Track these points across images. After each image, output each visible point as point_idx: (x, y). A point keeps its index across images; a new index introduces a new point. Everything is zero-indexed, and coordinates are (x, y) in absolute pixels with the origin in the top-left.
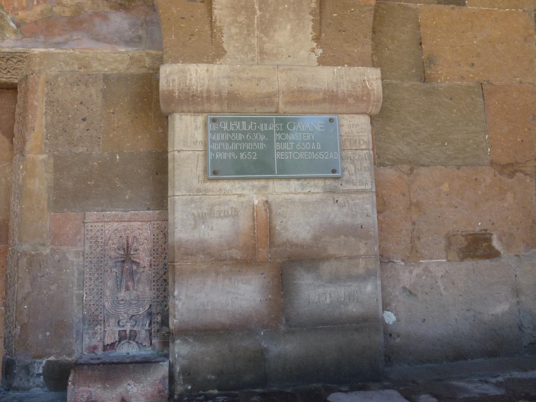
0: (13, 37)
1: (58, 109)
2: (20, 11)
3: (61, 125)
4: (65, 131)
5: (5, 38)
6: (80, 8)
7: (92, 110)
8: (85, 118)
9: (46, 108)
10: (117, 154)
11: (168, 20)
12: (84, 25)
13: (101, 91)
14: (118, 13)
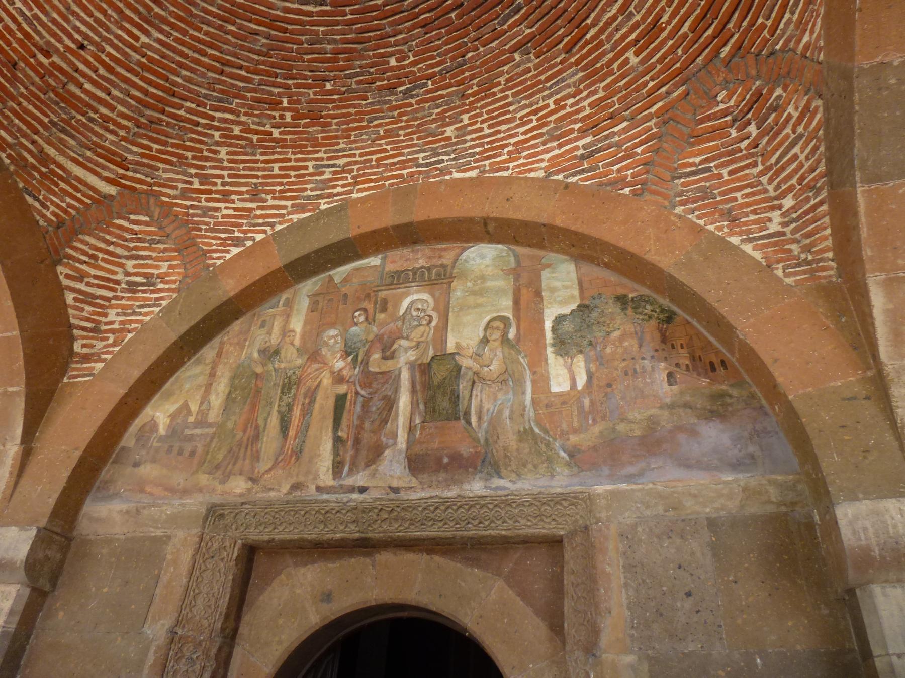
0: (566, 471)
1: (644, 578)
3: (653, 604)
4: (661, 615)
5: (555, 474)
6: (653, 423)
8: (690, 591)
9: (625, 577)
10: (757, 656)
11: (820, 431)
14: (711, 424)
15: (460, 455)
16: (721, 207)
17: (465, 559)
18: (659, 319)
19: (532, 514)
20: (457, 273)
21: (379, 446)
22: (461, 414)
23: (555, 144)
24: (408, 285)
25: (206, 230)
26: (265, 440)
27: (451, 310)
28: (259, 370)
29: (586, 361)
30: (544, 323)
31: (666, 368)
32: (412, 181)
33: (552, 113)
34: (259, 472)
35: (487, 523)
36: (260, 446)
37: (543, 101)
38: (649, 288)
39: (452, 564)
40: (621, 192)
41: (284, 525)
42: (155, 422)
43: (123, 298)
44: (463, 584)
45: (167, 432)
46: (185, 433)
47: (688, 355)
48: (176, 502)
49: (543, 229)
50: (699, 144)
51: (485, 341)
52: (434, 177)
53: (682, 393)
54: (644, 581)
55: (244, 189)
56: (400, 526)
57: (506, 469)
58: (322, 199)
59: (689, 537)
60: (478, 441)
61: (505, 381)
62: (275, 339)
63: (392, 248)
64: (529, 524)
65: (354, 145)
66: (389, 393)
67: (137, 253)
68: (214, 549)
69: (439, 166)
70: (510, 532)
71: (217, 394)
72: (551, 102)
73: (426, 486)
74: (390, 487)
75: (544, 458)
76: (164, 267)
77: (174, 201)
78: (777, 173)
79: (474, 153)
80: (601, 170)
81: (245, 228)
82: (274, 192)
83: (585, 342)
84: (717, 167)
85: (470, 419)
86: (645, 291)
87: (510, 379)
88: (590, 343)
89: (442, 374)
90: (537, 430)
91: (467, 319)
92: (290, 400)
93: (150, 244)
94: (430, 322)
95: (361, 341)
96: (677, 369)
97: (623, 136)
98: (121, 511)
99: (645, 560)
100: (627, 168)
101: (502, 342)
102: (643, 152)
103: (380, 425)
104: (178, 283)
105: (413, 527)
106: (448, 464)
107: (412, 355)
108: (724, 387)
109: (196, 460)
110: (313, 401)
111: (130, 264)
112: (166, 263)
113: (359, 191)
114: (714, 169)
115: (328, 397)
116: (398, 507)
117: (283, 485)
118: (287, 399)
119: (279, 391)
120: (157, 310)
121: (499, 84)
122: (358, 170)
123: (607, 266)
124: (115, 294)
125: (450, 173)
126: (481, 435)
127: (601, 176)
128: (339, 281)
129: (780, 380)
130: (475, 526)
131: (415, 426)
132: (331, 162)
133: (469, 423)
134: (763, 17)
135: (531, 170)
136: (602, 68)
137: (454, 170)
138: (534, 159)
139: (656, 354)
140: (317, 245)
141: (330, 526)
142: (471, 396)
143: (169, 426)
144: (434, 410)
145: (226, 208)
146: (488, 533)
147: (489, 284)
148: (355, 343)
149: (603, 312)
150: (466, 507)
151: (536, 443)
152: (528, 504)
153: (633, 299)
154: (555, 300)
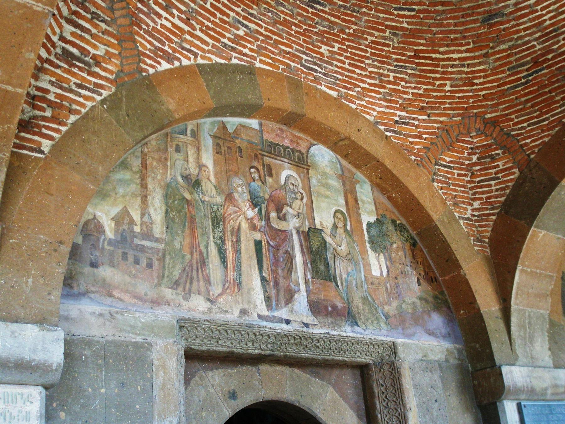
23: (385, 104)
25: (146, 32)
26: (211, 266)
28: (188, 196)
33: (390, 83)
36: (207, 271)
37: (388, 71)
38: (408, 221)
39: (304, 375)
42: (98, 221)
43: (58, 67)
44: (312, 388)
45: (115, 235)
46: (135, 242)
50: (453, 152)
51: (335, 226)
55: (183, 8)
60: (344, 299)
65: (262, 17)
66: (289, 249)
67: (77, 19)
69: (315, 74)
71: (155, 210)
72: (392, 75)
75: (375, 317)
76: (101, 51)
78: (477, 187)
81: (174, 45)
82: (202, 24)
86: (404, 222)
90: (370, 299)
91: (323, 205)
92: (221, 234)
93: (93, 18)
94: (302, 199)
97: (421, 124)
100: (417, 143)
103: (287, 273)
104: (114, 75)
109: (155, 274)
110: (239, 241)
111: (68, 28)
112: (102, 47)
113: (261, 61)
117: (234, 310)
119: (210, 224)
120: (99, 98)
121: (366, 39)
122: (262, 41)
123: (390, 198)
124: (48, 56)
125: (321, 85)
126: (344, 295)
129: (478, 301)
132: (246, 22)
133: (337, 285)
134: (516, 116)
135: (368, 113)
136: (429, 78)
137: (323, 83)
138: (370, 106)
142: (335, 266)
143: (116, 231)
145: (166, 18)
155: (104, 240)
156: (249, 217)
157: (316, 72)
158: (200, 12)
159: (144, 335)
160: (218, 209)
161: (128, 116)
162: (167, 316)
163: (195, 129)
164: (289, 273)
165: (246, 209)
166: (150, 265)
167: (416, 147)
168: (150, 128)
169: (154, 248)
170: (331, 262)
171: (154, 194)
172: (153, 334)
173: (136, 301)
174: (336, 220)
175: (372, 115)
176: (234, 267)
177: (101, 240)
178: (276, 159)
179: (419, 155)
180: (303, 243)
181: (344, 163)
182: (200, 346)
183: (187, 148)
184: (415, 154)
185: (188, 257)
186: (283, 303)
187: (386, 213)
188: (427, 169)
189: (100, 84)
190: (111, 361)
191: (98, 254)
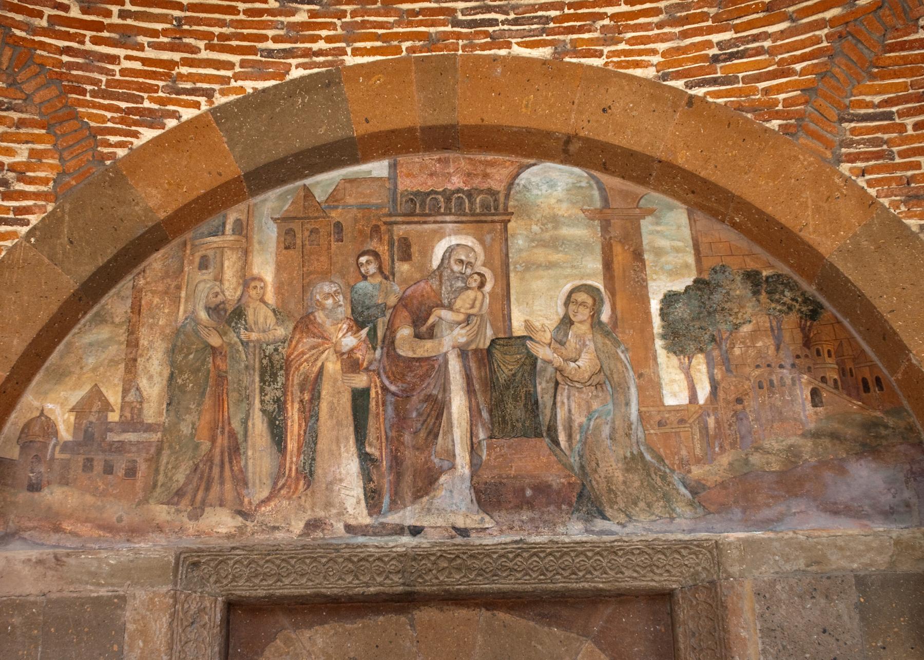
0: (688, 512)
1: (784, 644)
2: (693, 465)
5: (675, 515)
6: (795, 456)
7: (846, 644)
9: (763, 643)
12: (807, 486)
13: (856, 608)
14: (862, 462)
15: (550, 486)
16: (898, 174)
17: (539, 615)
18: (802, 312)
19: (641, 563)
20: (515, 207)
21: (429, 469)
22: (544, 429)
23: (677, 30)
24: (439, 218)
25: (94, 94)
26: (250, 453)
27: (512, 268)
29: (708, 364)
30: (649, 302)
31: (810, 383)
32: (446, 47)
34: (250, 503)
35: (581, 574)
36: (243, 463)
38: (791, 266)
39: (523, 622)
40: (768, 125)
41: (293, 576)
42: (47, 417)
44: (539, 647)
47: (836, 366)
48: (124, 547)
49: (656, 165)
51: (567, 322)
52: (483, 47)
53: (828, 418)
54: (784, 647)
55: (159, 26)
56: (464, 576)
57: (612, 508)
58: (293, 58)
59: (835, 597)
60: (572, 469)
61: (599, 386)
62: (231, 290)
63: (408, 152)
64: (635, 575)
66: (435, 392)
68: (192, 612)
69: (491, 29)
70: (610, 584)
71: (150, 378)
73: (504, 527)
74: (454, 528)
76: (22, 154)
77: (37, 38)
79: (547, 17)
80: (741, 85)
81: (161, 94)
82: (208, 36)
83: (707, 337)
84: (901, 114)
85: (557, 436)
86: (785, 270)
87: (607, 382)
88: (713, 339)
89: (510, 367)
90: (648, 457)
91: (539, 284)
92: (279, 394)
94: (482, 285)
95: (377, 306)
96: (824, 385)
97: (779, 43)
98: (29, 560)
99: (786, 624)
100: (779, 89)
101: (592, 326)
102: (803, 72)
103: (426, 439)
104: (51, 184)
105: (481, 578)
106: (534, 497)
107: (460, 335)
108: (878, 414)
109: (139, 484)
110: (316, 397)
112: (25, 146)
113: (356, 52)
114: (896, 116)
115: (339, 392)
116: (464, 553)
117: (293, 523)
118: (272, 392)
119: (257, 379)
120: (24, 230)
122: (354, 14)
123: (734, 225)
125: (508, 45)
126: (574, 460)
127: (739, 92)
128: (323, 198)
130: (565, 578)
131: (479, 442)
133: (556, 443)
135: (637, 65)
137: (514, 41)
138: (642, 47)
139: (797, 361)
140: (298, 145)
141: (361, 578)
142: (555, 403)
143: (77, 427)
144: (504, 422)
145: (128, 58)
146: (581, 585)
147: (565, 231)
148: (368, 308)
149: (728, 293)
150: (558, 555)
151: (649, 475)
152: (638, 551)
153: (767, 278)
154: (662, 268)
155: (55, 446)
156: (345, 350)
157: (492, 26)
158: (198, 18)
159: (113, 585)
160: (276, 350)
161: (71, 242)
162: (155, 550)
163: (243, 217)
164: (431, 437)
165: (340, 335)
166: (131, 472)
167: (782, 97)
168: (109, 251)
169: (143, 442)
170: (545, 399)
171: (151, 353)
172: (129, 582)
173: (101, 533)
174: (572, 307)
175: (647, 65)
176: (299, 449)
177: (50, 447)
178: (425, 223)
179: (788, 112)
180: (474, 372)
181: (605, 178)
182: (243, 589)
183: (222, 256)
184: (778, 115)
185: (206, 445)
186: (408, 496)
187: (727, 261)
188: (819, 138)
189: (24, 207)
190: (52, 630)
191: (42, 470)
